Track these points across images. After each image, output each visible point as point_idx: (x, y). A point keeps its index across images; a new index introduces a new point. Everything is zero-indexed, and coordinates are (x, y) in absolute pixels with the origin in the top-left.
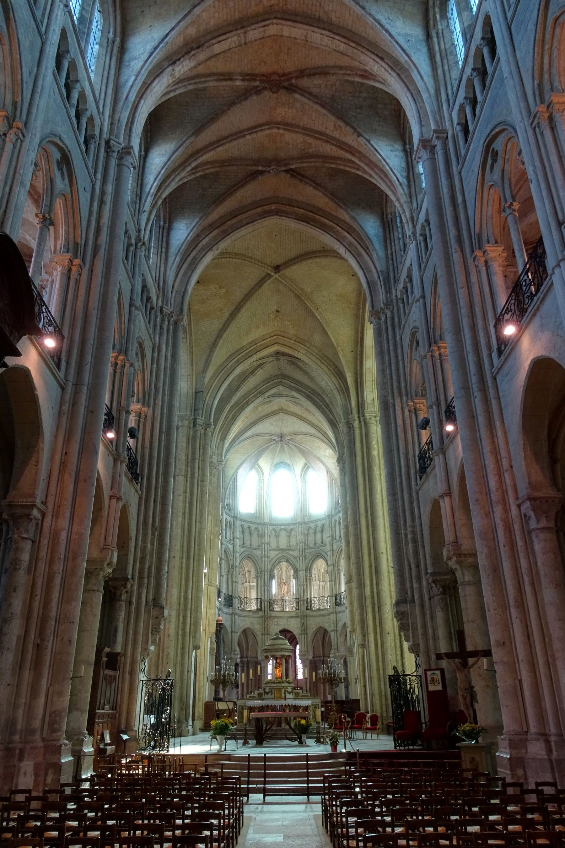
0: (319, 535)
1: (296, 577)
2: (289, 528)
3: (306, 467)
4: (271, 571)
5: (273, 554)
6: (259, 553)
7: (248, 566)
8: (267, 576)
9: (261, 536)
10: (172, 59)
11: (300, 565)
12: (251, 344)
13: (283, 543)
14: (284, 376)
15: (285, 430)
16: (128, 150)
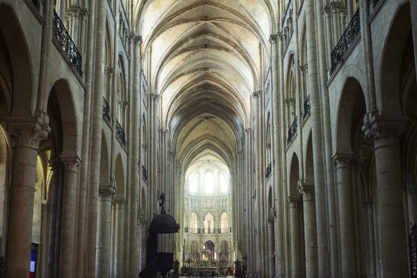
0: (224, 202)
1: (214, 220)
2: (211, 199)
3: (219, 173)
4: (204, 217)
5: (204, 210)
6: (198, 210)
7: (193, 214)
8: (202, 219)
9: (199, 202)
10: (176, 97)
11: (216, 215)
12: (197, 139)
13: (209, 206)
14: (209, 144)
15: (210, 159)
16: (167, 130)
